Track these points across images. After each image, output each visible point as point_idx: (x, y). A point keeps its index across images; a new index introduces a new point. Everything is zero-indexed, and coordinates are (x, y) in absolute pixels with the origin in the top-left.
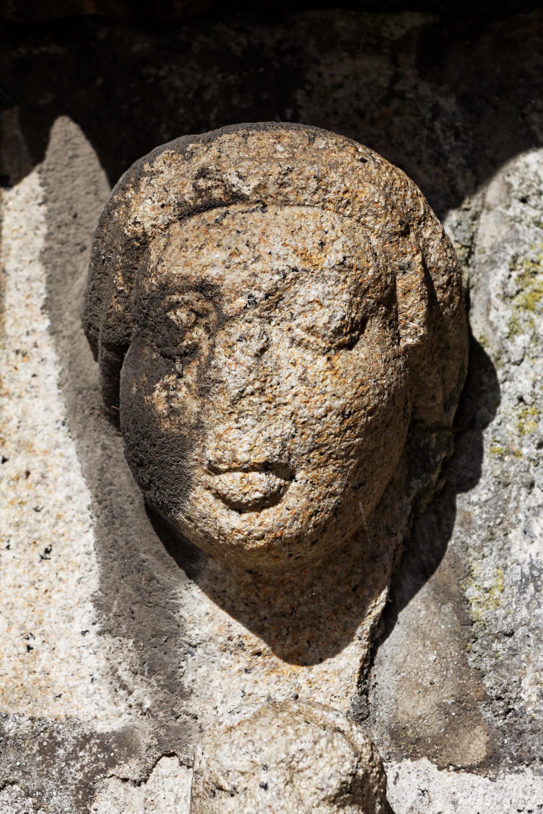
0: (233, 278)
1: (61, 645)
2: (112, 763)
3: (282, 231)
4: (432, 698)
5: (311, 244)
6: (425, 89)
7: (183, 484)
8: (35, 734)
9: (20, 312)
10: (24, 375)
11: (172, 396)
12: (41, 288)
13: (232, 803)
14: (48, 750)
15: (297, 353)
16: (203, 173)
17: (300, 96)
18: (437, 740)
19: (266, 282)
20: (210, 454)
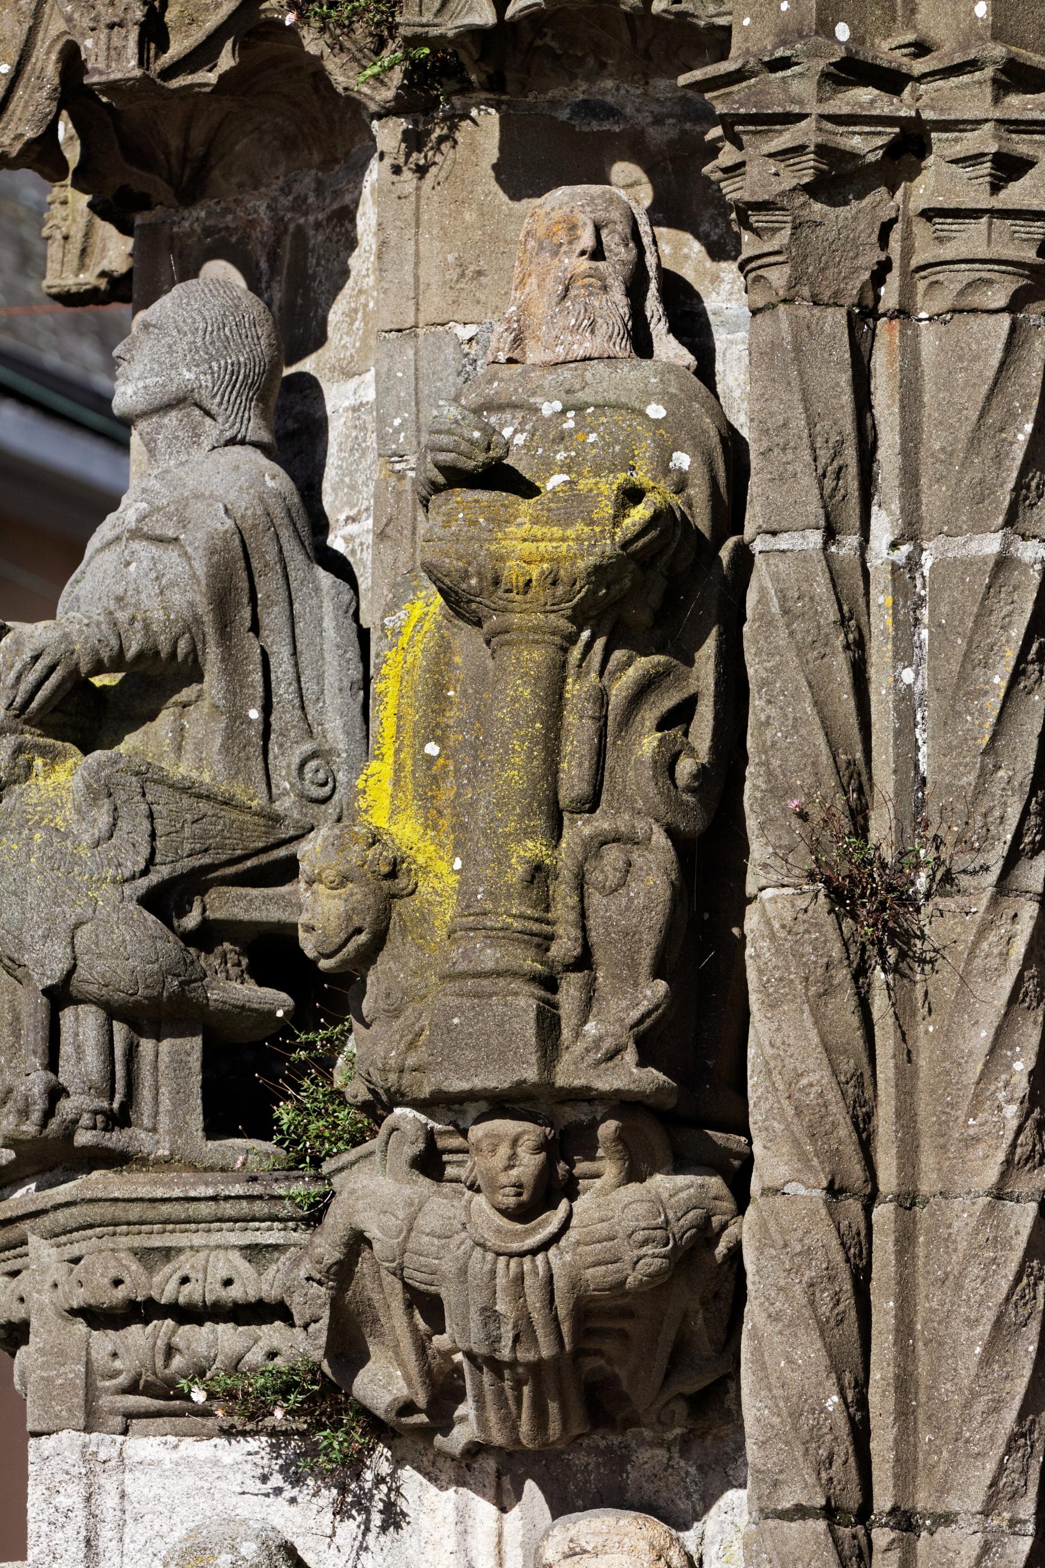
6: (682, 1463)
16: (571, 1541)
17: (629, 1467)
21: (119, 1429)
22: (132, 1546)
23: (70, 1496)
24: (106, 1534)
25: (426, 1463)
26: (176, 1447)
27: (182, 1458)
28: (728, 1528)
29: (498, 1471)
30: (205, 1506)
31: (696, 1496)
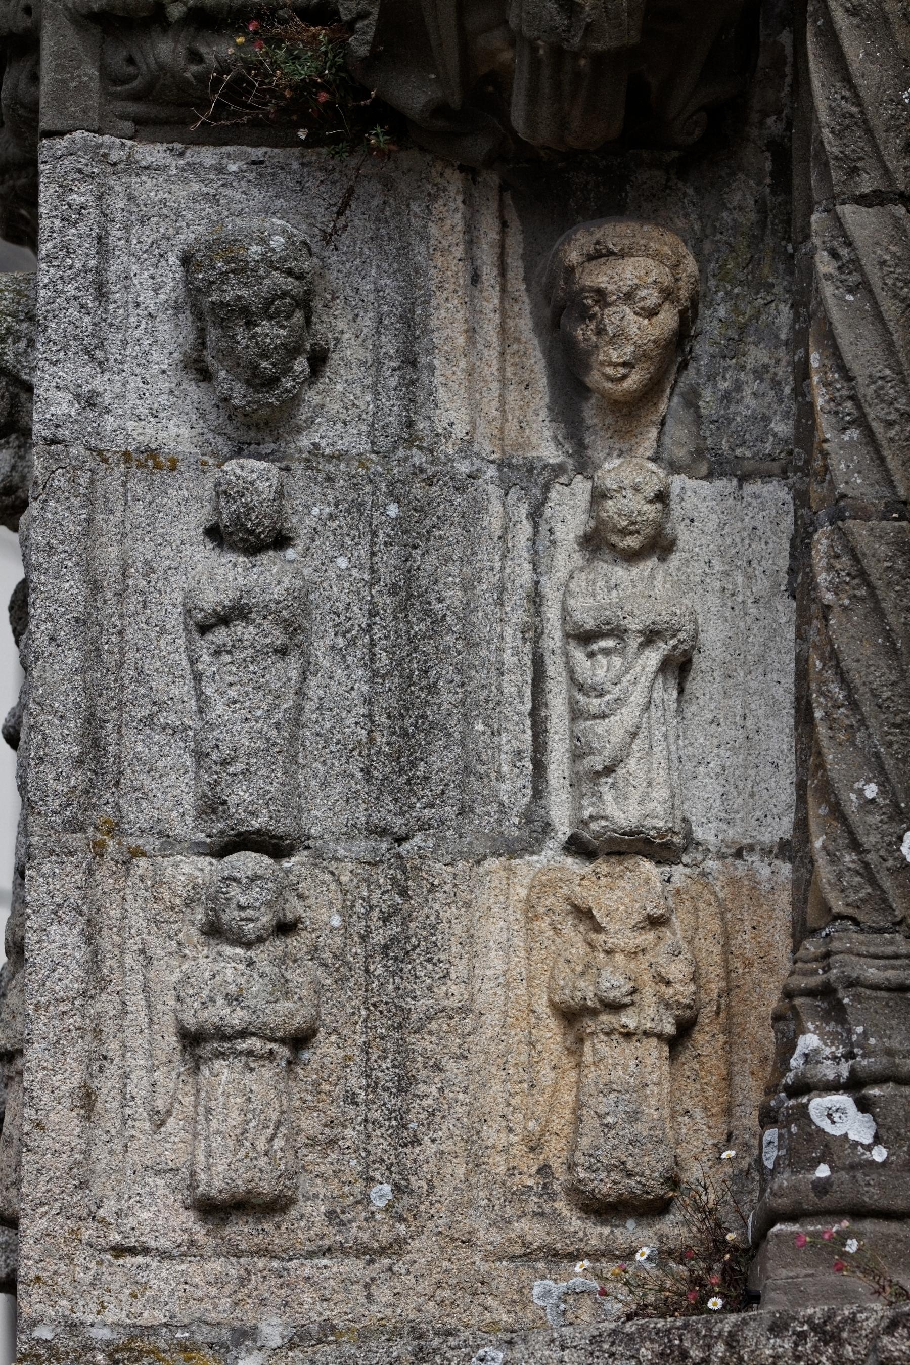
0: (611, 288)
1: (534, 425)
2: (557, 477)
3: (631, 268)
4: (685, 449)
5: (642, 273)
6: (680, 184)
7: (588, 368)
8: (525, 464)
9: (514, 281)
10: (516, 309)
11: (583, 333)
12: (521, 271)
13: (610, 502)
14: (530, 470)
15: (636, 318)
16: (598, 243)
17: (628, 187)
18: (688, 466)
19: (625, 289)
20: (601, 358)
21: (130, 132)
22: (138, 246)
23: (83, 195)
24: (116, 232)
25: (434, 173)
26: (182, 154)
27: (188, 164)
28: (724, 248)
29: (500, 186)
30: (211, 211)
31: (693, 216)
